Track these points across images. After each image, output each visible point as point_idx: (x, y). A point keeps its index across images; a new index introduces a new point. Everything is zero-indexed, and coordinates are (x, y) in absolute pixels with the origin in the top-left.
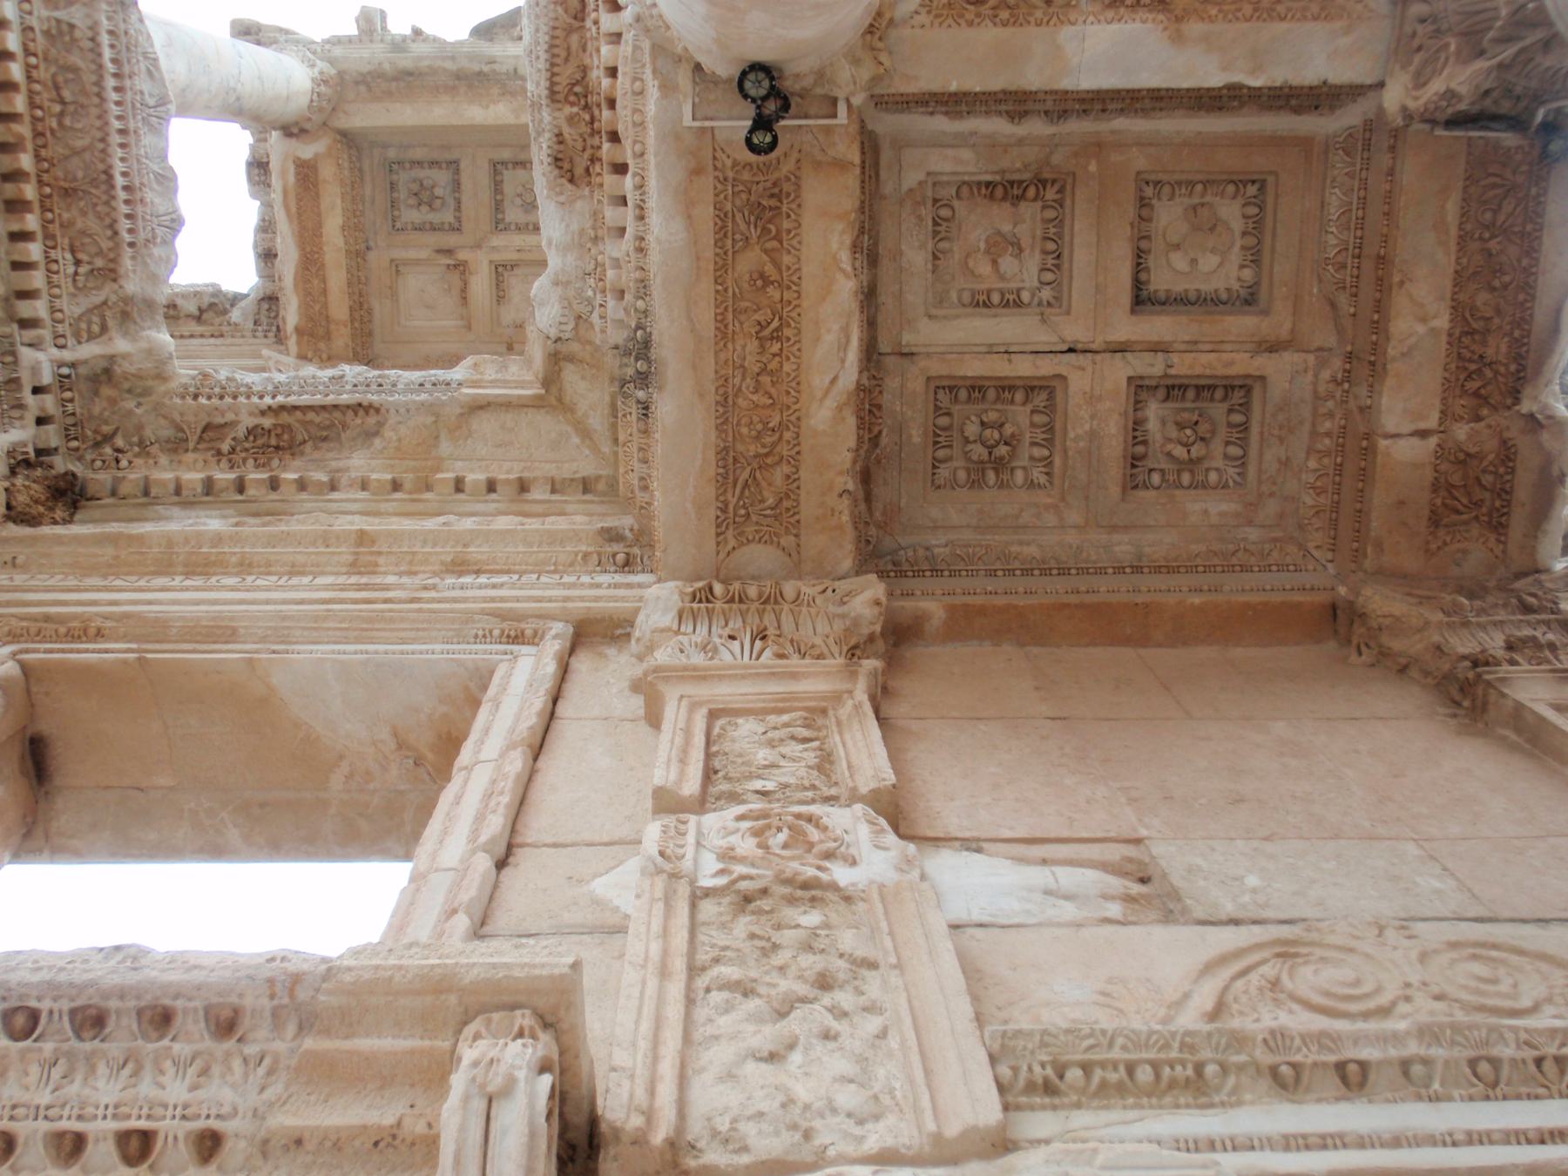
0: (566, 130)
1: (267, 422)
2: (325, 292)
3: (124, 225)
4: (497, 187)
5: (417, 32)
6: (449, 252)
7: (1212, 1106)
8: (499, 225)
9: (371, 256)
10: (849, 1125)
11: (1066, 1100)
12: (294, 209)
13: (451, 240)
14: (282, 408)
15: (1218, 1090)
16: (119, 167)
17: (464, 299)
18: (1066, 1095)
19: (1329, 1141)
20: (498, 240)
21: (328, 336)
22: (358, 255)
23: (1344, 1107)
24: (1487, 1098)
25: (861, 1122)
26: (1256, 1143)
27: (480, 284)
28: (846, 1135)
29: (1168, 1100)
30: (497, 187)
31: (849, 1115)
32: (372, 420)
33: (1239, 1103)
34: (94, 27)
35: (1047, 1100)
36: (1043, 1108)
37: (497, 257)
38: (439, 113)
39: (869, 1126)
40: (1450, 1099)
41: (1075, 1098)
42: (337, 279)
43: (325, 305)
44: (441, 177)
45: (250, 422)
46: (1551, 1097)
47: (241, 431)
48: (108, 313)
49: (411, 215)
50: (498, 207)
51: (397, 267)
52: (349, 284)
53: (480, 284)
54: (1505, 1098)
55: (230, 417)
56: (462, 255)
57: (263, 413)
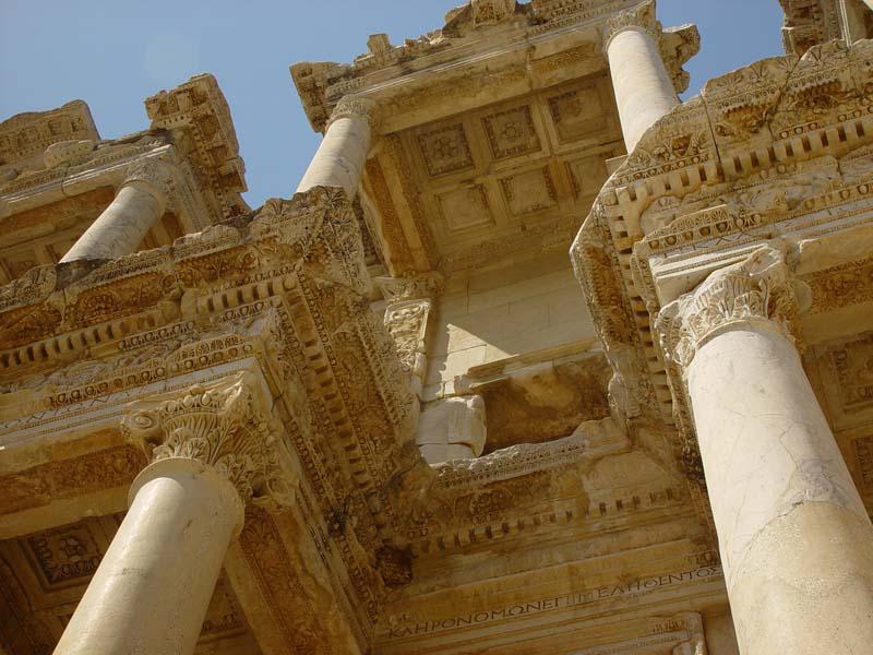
0: (614, 318)
1: (489, 491)
2: (403, 234)
3: (391, 416)
4: (489, 131)
5: (411, 44)
6: (470, 181)
8: (497, 155)
9: (423, 197)
12: (371, 190)
13: (470, 174)
14: (495, 482)
16: (382, 390)
17: (486, 204)
20: (498, 167)
21: (412, 260)
22: (414, 203)
27: (495, 195)
30: (489, 131)
32: (543, 478)
34: (355, 329)
37: (501, 176)
38: (445, 109)
42: (408, 224)
43: (406, 241)
44: (453, 135)
45: (479, 493)
47: (476, 498)
48: (394, 459)
49: (439, 164)
50: (493, 144)
51: (439, 198)
52: (416, 224)
53: (495, 195)
55: (469, 492)
56: (479, 181)
57: (485, 486)
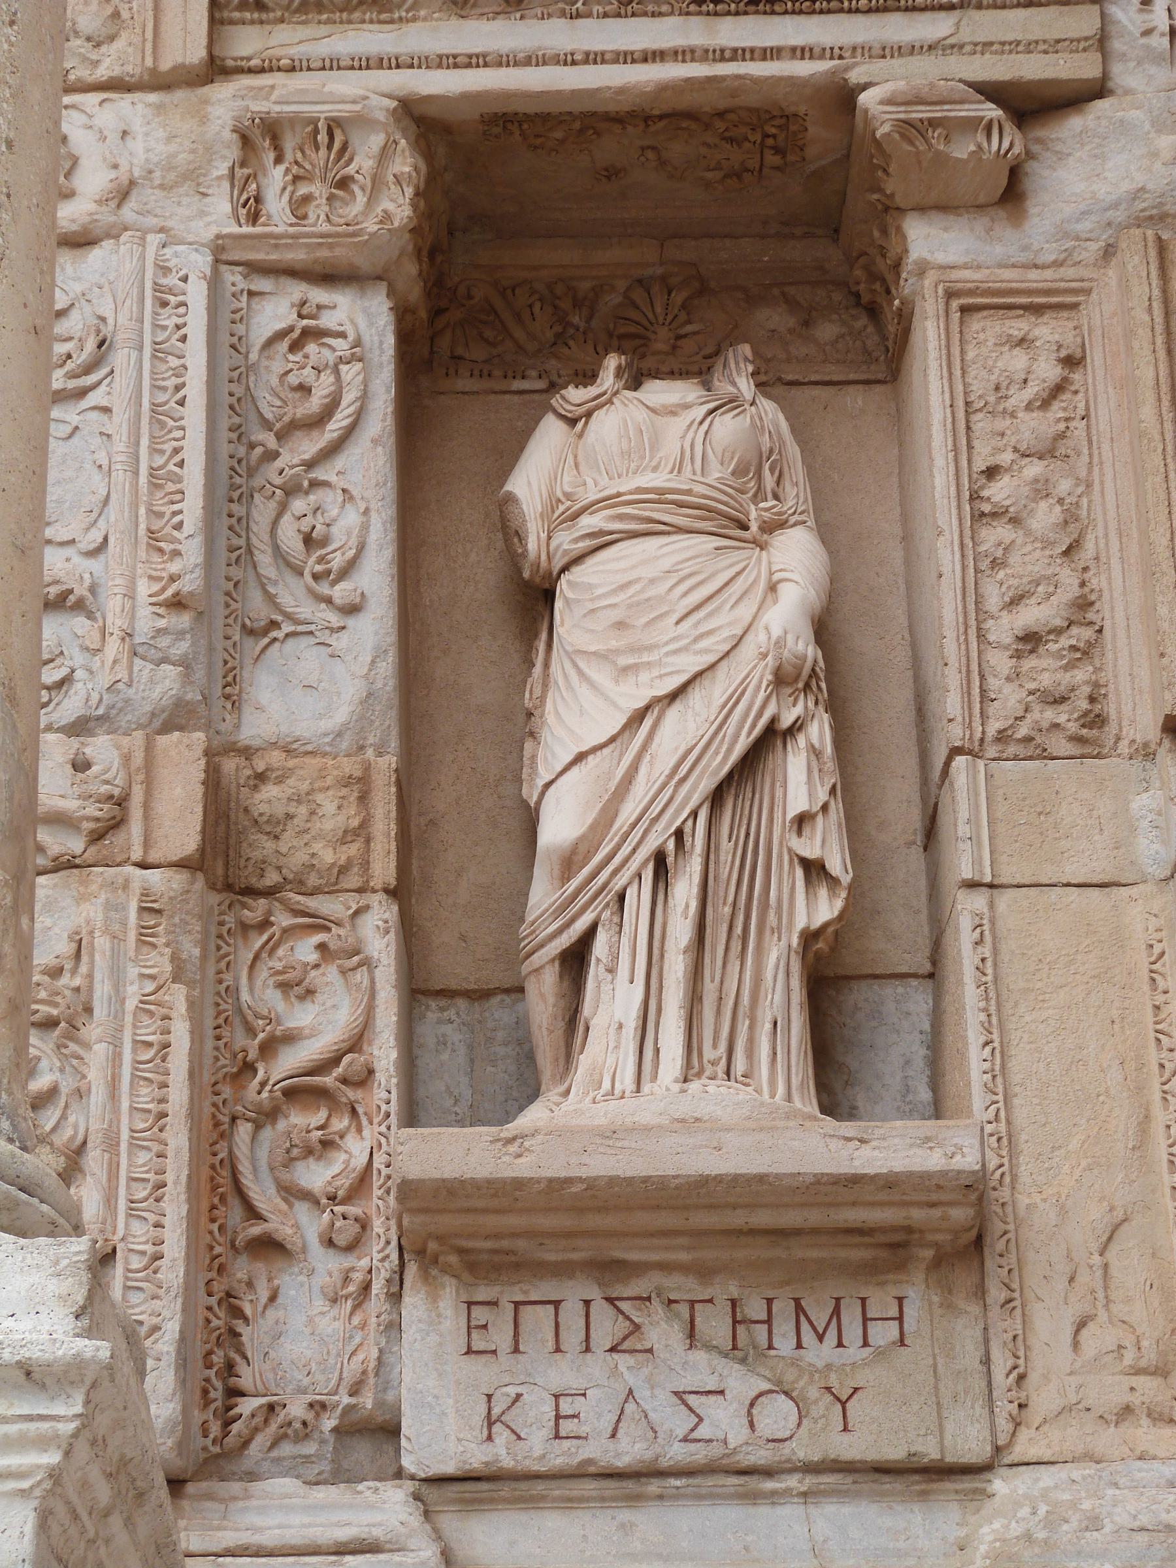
7: (392, 22)
10: (85, 48)
11: (271, 15)
15: (399, 7)
18: (273, 11)
19: (474, 61)
23: (499, 24)
24: (619, 15)
25: (98, 45)
26: (416, 61)
28: (84, 59)
29: (357, 15)
31: (88, 39)
33: (414, 19)
35: (256, 15)
36: (252, 22)
39: (104, 49)
40: (589, 15)
41: (279, 13)
46: (672, 13)
54: (633, 15)
